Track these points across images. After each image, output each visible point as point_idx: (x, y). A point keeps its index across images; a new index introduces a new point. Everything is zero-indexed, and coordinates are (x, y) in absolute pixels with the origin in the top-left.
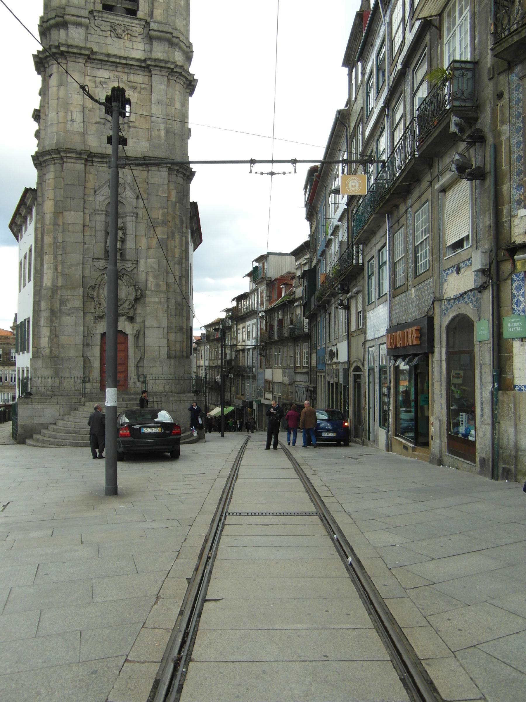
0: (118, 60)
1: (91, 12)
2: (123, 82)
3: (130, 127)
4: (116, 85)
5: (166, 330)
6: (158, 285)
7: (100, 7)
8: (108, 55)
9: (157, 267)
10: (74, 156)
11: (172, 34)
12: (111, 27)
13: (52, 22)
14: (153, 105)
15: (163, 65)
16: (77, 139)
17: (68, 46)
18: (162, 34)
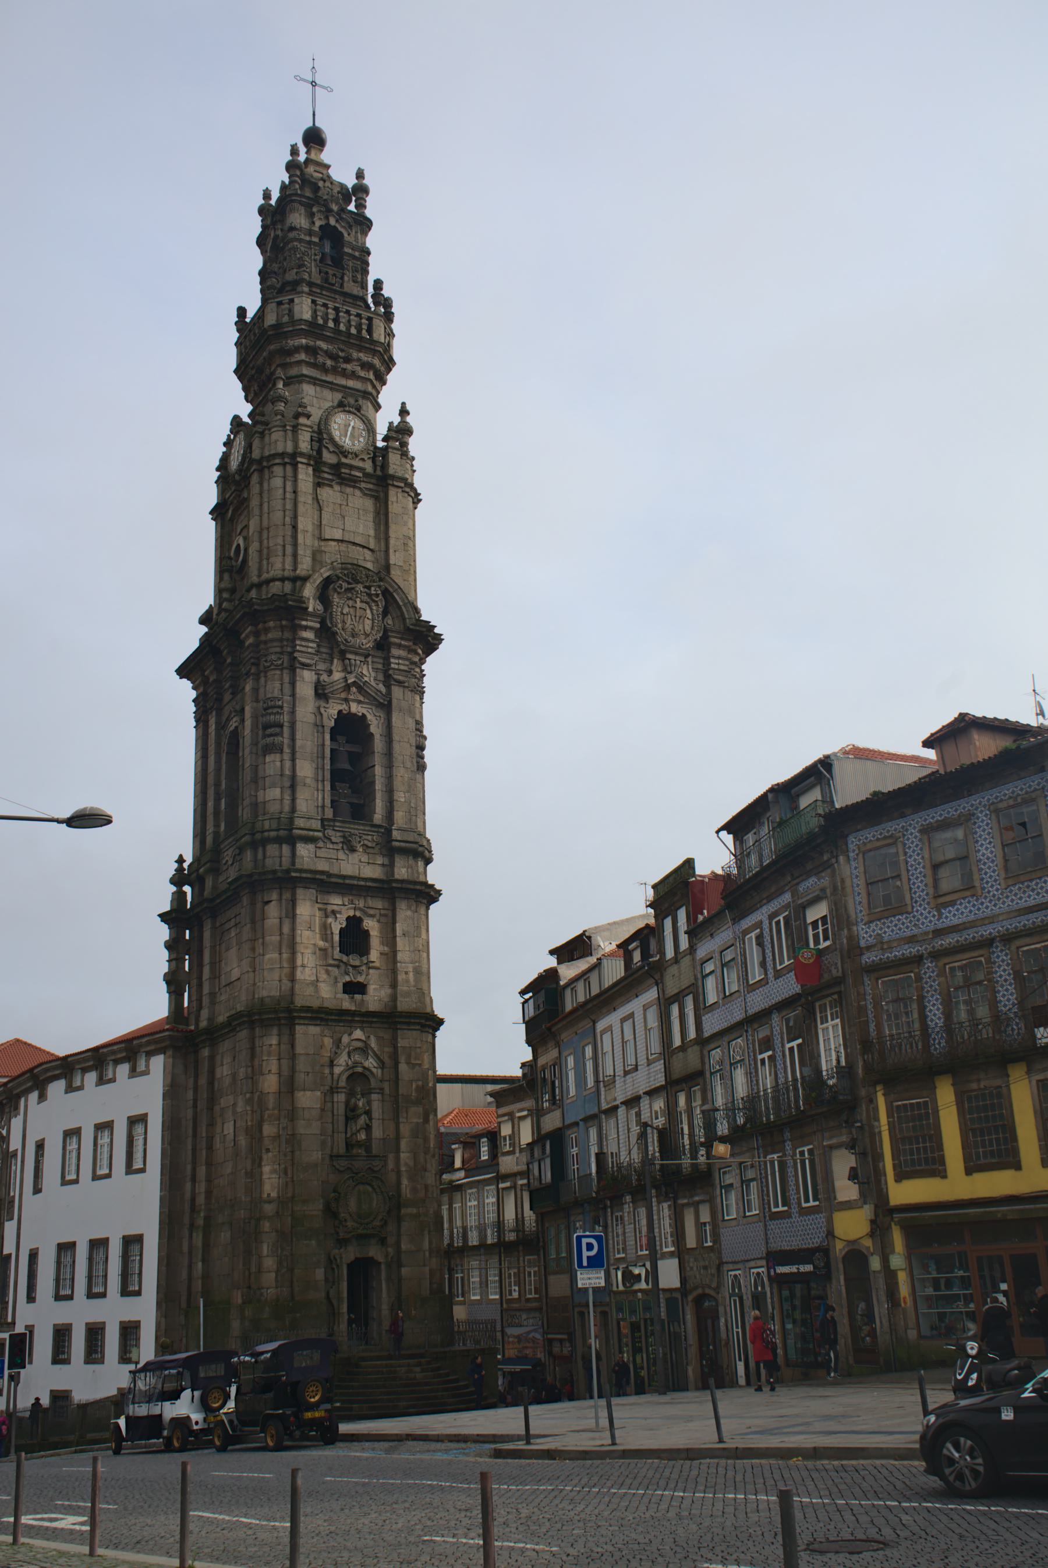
0: (355, 882)
1: (322, 820)
2: (360, 909)
3: (369, 968)
4: (351, 913)
5: (427, 1254)
6: (414, 1190)
7: (329, 813)
8: (344, 877)
9: (411, 1164)
10: (309, 1015)
11: (416, 843)
12: (344, 837)
13: (273, 834)
14: (398, 939)
15: (412, 887)
16: (310, 990)
17: (301, 871)
18: (407, 845)
